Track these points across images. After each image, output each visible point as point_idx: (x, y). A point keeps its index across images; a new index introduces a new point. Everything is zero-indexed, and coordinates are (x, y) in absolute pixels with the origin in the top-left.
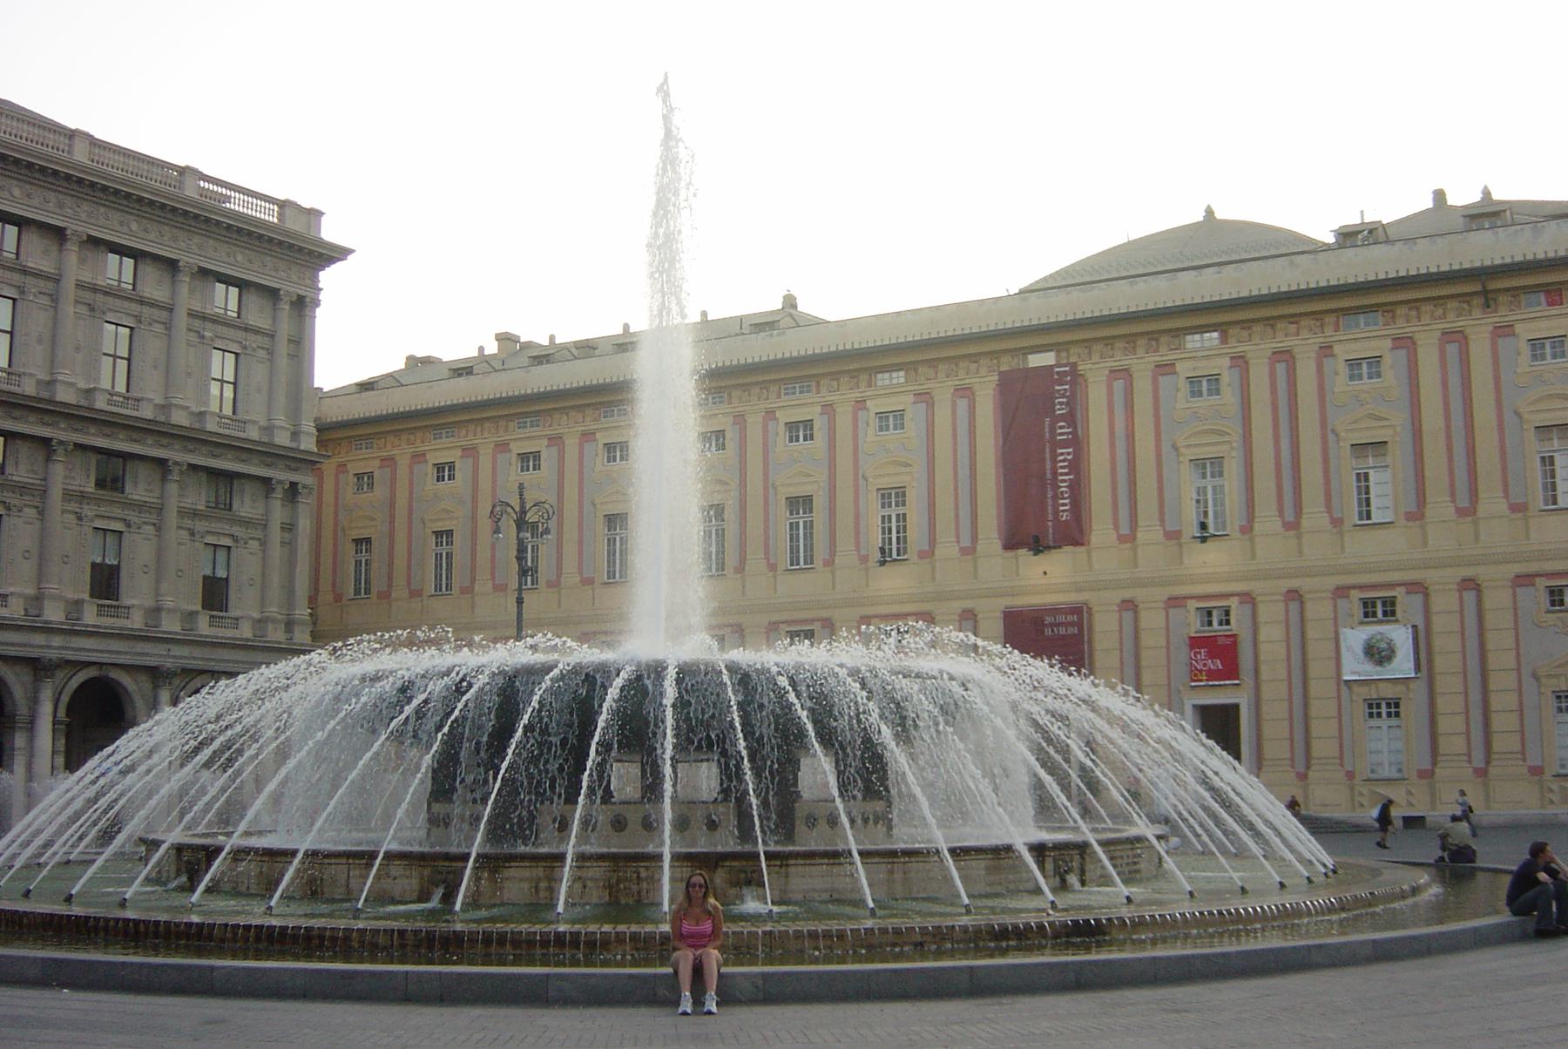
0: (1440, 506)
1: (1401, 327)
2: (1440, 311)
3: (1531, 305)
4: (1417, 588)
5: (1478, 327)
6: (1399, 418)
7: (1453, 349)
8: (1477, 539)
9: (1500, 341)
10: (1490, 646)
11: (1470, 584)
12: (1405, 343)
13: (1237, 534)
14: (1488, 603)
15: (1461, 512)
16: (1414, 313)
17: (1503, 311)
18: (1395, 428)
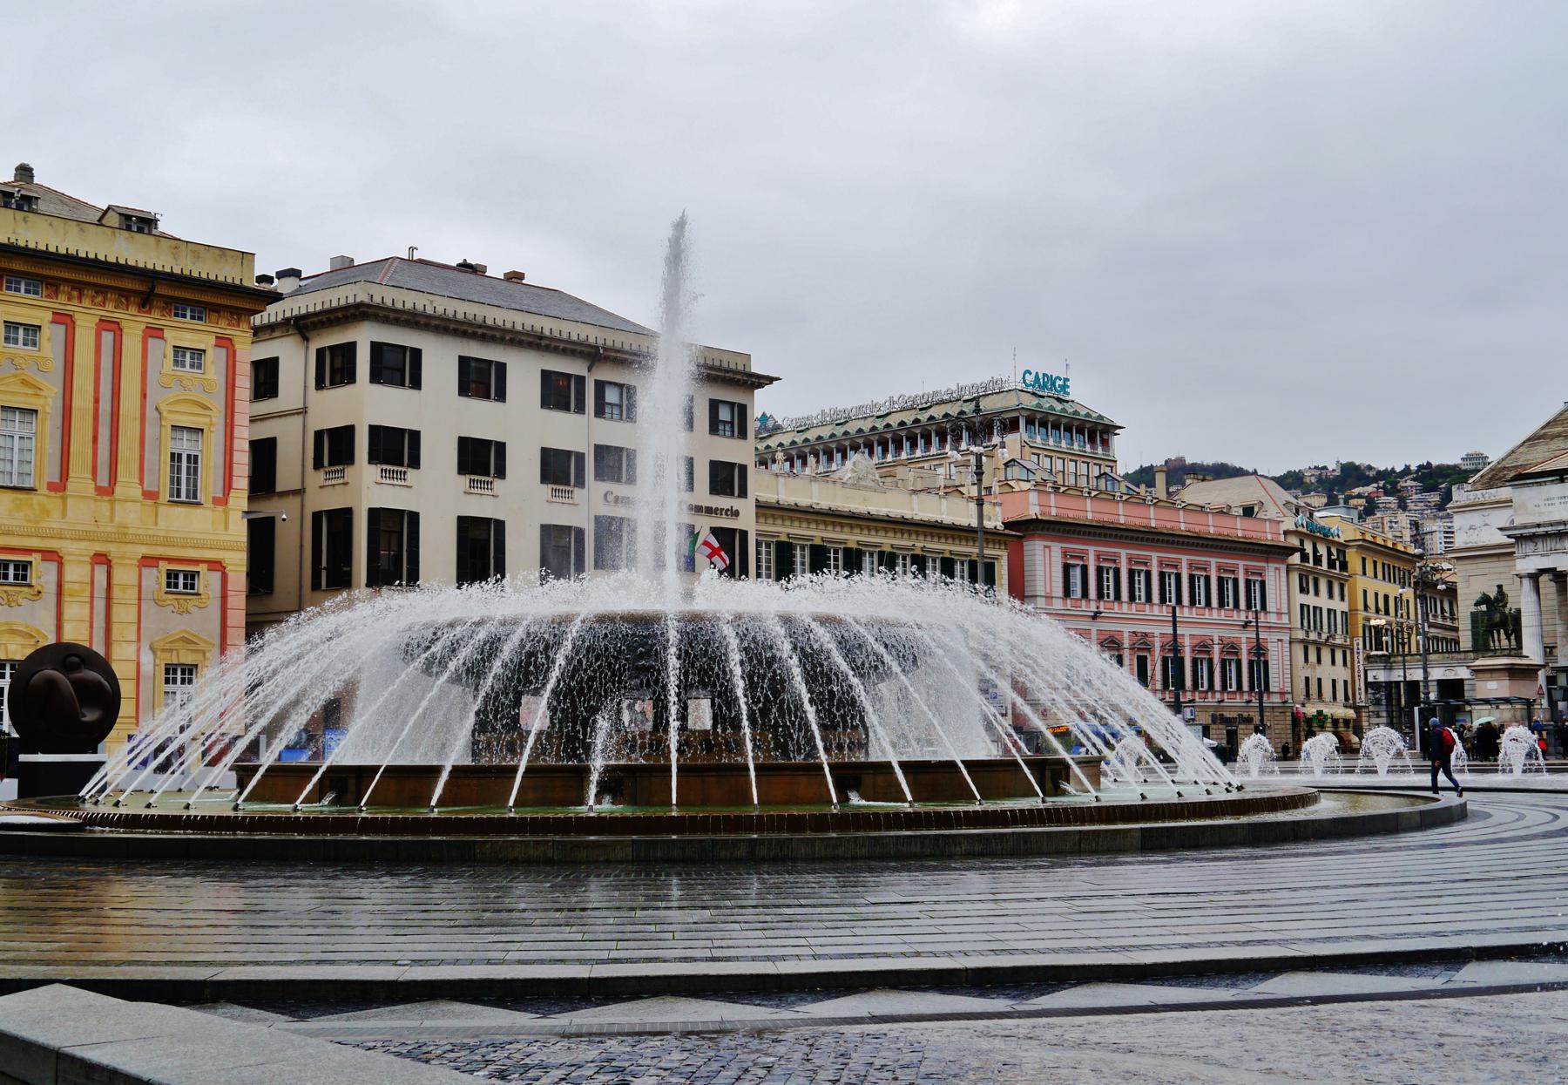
0: (80, 480)
1: (62, 303)
2: (100, 299)
3: (176, 315)
4: (50, 555)
5: (134, 323)
6: (53, 390)
7: (108, 338)
8: (112, 518)
9: (150, 340)
10: (115, 618)
11: (101, 559)
12: (65, 320)
13: (209, 504)
14: (115, 581)
15: (100, 491)
16: (75, 293)
17: (156, 314)
18: (50, 403)
